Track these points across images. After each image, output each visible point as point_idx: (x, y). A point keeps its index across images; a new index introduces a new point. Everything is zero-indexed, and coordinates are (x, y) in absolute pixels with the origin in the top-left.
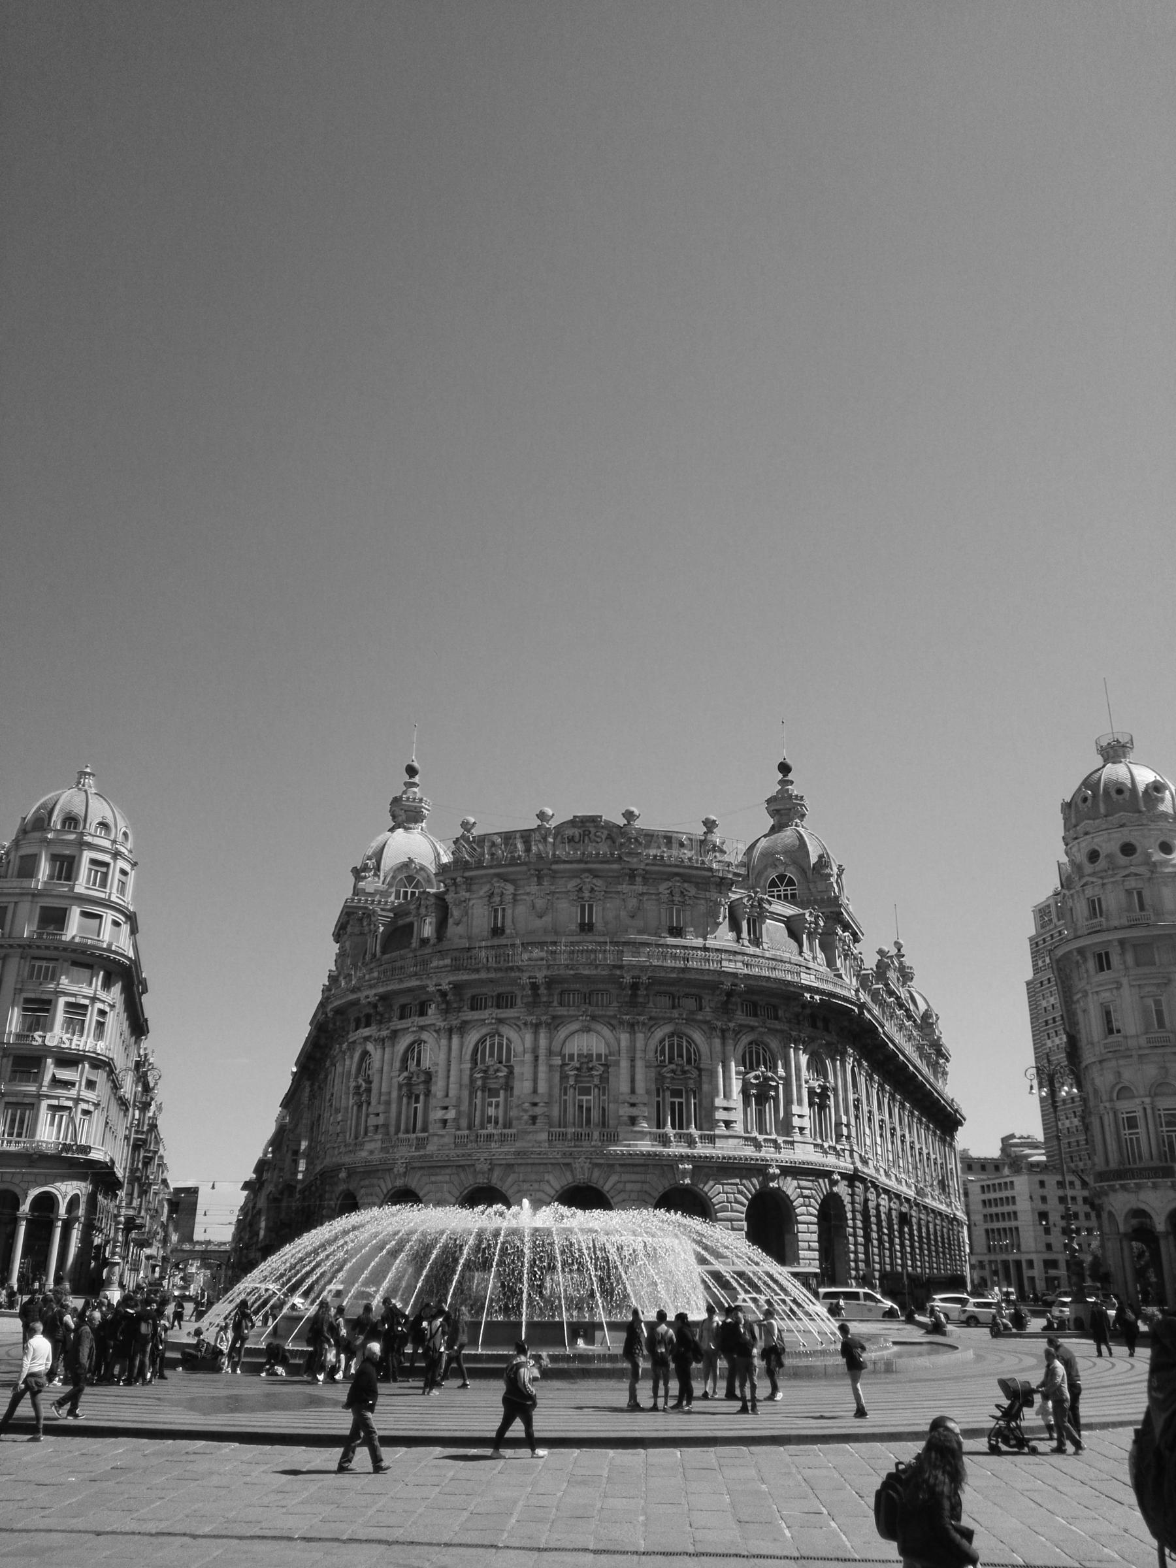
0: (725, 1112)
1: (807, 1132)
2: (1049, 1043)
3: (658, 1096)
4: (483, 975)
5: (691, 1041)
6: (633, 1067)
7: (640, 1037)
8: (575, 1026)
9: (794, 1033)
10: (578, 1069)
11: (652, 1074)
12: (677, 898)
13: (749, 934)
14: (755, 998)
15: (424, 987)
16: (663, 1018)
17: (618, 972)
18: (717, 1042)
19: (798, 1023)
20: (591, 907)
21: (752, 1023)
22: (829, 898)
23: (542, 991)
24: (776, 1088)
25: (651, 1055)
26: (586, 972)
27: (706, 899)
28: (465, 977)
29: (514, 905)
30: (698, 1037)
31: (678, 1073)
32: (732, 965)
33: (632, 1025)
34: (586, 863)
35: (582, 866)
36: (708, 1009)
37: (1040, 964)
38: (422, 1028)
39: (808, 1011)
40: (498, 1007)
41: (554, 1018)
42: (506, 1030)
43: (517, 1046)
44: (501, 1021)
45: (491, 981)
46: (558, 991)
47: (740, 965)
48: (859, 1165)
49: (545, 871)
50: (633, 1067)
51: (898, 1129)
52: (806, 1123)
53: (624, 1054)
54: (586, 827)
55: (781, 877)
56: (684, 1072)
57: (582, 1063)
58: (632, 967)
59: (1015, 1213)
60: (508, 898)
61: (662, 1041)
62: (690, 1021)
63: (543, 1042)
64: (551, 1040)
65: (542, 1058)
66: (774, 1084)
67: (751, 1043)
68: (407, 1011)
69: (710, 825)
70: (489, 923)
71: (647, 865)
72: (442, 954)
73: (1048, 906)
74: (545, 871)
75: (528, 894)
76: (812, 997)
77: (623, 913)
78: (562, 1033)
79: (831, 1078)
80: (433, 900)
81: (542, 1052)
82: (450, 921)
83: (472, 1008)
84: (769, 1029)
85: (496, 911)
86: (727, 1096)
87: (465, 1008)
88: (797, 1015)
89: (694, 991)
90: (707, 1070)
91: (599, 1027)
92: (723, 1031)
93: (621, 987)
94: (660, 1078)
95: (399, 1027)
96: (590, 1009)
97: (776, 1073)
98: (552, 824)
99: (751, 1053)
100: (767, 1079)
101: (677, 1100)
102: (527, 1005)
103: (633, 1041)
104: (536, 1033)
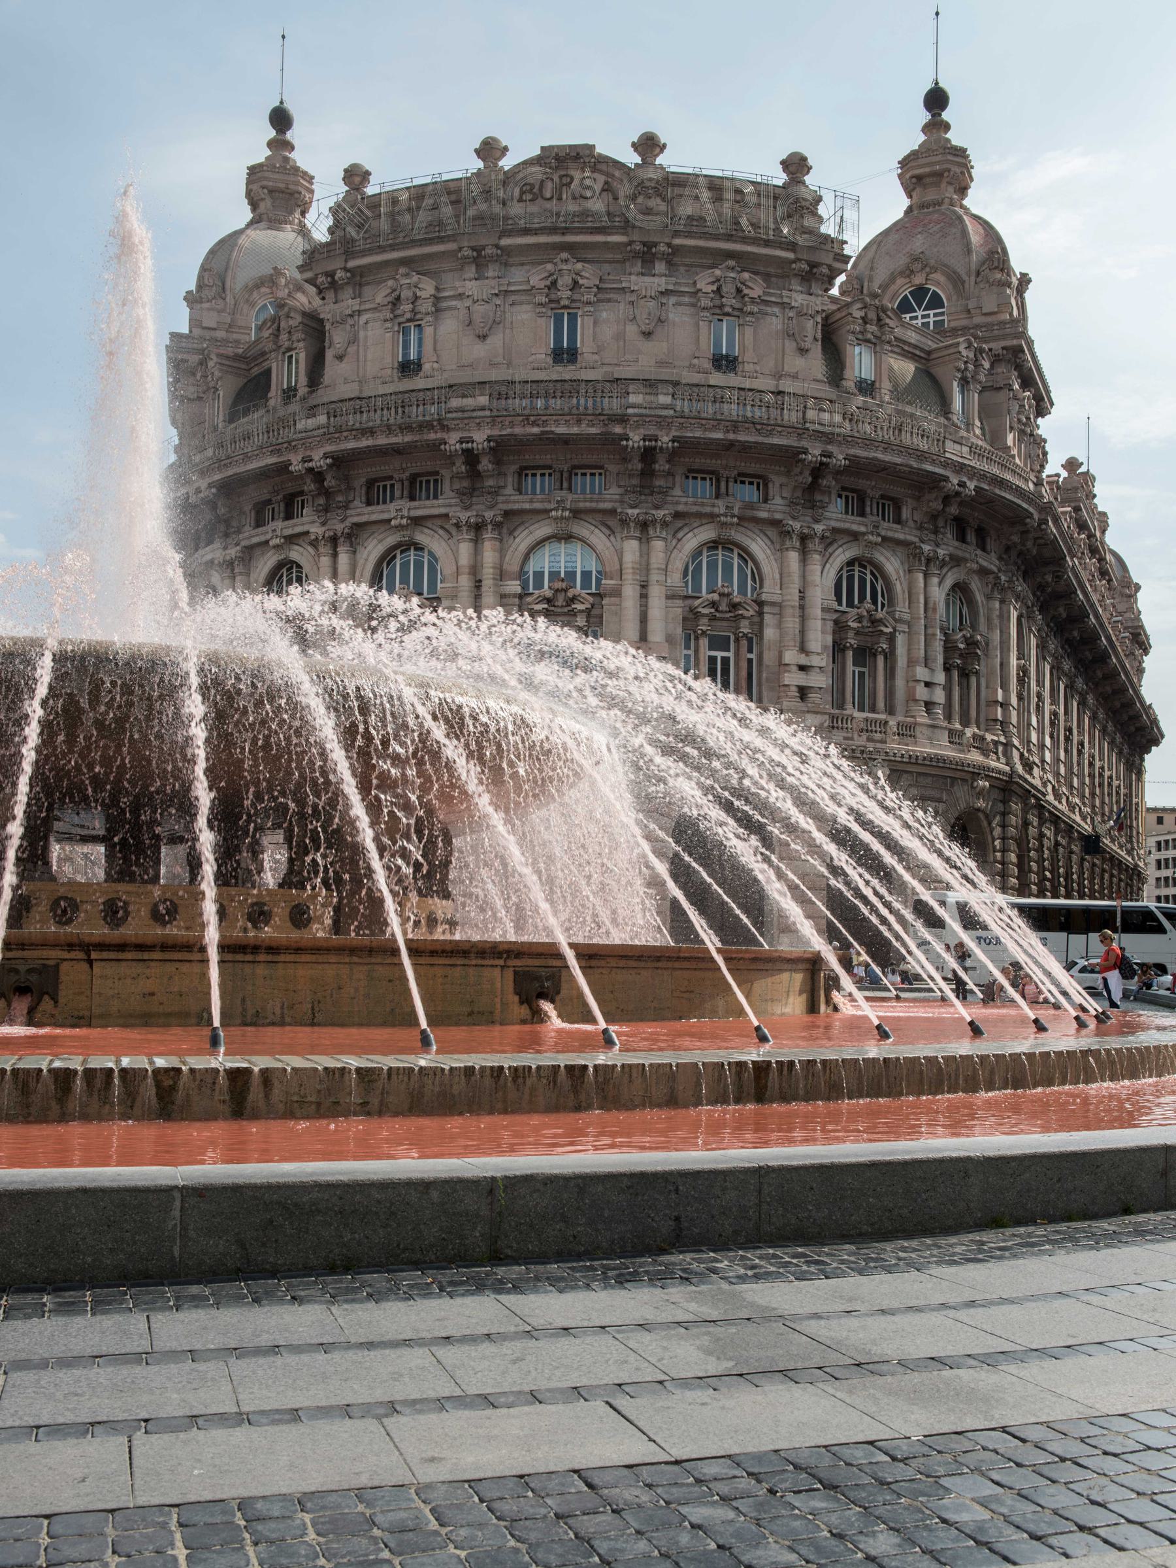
0: (802, 675)
3: (688, 647)
4: (382, 440)
5: (746, 555)
6: (644, 596)
7: (658, 545)
8: (543, 529)
9: (926, 548)
10: (548, 601)
11: (678, 609)
12: (730, 301)
14: (862, 484)
15: (283, 468)
16: (699, 515)
17: (618, 430)
18: (793, 557)
19: (936, 532)
20: (573, 319)
21: (855, 527)
22: (1002, 323)
23: (485, 465)
24: (891, 639)
25: (675, 579)
26: (561, 430)
27: (783, 305)
28: (351, 445)
29: (437, 319)
30: (759, 547)
33: (644, 526)
34: (565, 231)
35: (557, 239)
36: (778, 500)
38: (291, 539)
39: (954, 510)
40: (412, 498)
41: (507, 514)
42: (422, 537)
43: (446, 566)
44: (417, 521)
45: (397, 451)
47: (838, 418)
48: (1019, 768)
49: (489, 251)
50: (644, 596)
51: (1075, 732)
52: (939, 696)
53: (628, 576)
54: (566, 162)
55: (920, 293)
56: (734, 606)
57: (557, 591)
58: (642, 420)
60: (426, 307)
61: (697, 553)
62: (746, 520)
63: (489, 555)
64: (502, 553)
65: (488, 583)
66: (888, 630)
67: (850, 563)
68: (268, 514)
69: (796, 165)
70: (394, 354)
72: (312, 411)
74: (489, 251)
75: (460, 296)
76: (962, 484)
77: (631, 330)
78: (523, 540)
79: (983, 627)
80: (299, 319)
81: (488, 574)
82: (329, 354)
83: (369, 503)
84: (885, 539)
85: (406, 332)
86: (803, 649)
87: (357, 503)
88: (934, 517)
89: (754, 468)
90: (773, 604)
91: (581, 529)
92: (804, 538)
93: (624, 456)
94: (691, 617)
95: (255, 540)
96: (570, 497)
97: (891, 613)
98: (506, 163)
99: (850, 579)
100: (874, 622)
101: (719, 654)
102: (461, 493)
103: (645, 554)
104: (477, 541)
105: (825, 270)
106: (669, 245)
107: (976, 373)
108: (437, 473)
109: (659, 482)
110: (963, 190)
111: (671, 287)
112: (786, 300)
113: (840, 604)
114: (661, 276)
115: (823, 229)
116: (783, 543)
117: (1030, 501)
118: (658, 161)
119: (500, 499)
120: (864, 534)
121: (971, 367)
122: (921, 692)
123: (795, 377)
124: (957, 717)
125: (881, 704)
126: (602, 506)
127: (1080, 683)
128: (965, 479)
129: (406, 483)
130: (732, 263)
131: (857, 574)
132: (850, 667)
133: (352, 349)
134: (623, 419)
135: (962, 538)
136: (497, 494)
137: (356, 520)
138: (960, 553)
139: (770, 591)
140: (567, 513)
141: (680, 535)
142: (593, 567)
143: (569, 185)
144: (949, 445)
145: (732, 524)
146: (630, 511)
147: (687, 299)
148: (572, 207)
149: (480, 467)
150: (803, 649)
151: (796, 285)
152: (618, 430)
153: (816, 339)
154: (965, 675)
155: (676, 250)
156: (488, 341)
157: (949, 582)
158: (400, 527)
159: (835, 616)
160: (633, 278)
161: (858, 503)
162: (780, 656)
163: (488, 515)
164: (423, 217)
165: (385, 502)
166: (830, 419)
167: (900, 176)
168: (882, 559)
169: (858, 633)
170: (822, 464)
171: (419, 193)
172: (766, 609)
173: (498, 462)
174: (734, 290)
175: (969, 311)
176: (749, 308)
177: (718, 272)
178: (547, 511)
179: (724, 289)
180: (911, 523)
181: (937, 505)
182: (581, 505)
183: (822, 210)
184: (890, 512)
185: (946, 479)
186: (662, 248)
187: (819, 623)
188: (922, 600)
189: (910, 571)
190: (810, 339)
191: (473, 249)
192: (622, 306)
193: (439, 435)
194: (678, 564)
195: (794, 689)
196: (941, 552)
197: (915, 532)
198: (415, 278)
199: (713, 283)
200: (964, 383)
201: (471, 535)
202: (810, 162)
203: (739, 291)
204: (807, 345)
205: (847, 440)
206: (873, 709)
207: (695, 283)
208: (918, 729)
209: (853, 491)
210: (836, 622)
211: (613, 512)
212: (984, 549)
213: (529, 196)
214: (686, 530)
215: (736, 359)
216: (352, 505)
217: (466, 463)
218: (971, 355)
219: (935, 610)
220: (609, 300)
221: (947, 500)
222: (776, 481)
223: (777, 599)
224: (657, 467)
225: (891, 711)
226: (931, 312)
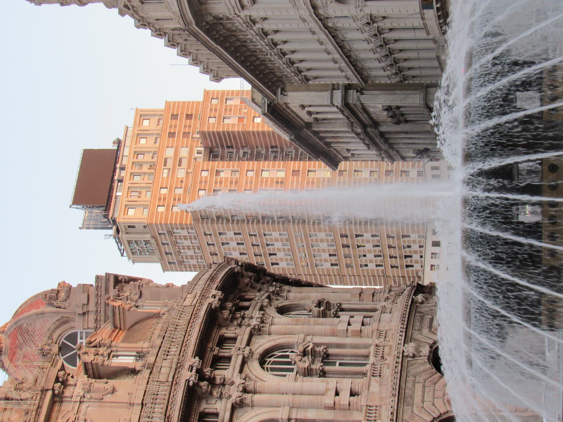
9: (254, 322)
18: (257, 397)
19: (243, 318)
21: (239, 361)
24: (317, 345)
37: (194, 262)
39: (229, 305)
47: (166, 364)
66: (311, 346)
67: (263, 368)
90: (290, 412)
92: (245, 391)
99: (273, 370)
100: (304, 353)
105: (62, 373)
107: (132, 300)
112: (78, 399)
122: (356, 326)
125: (363, 351)
128: (211, 295)
131: (269, 366)
132: (337, 367)
135: (247, 308)
144: (187, 302)
151: (67, 393)
157: (278, 315)
161: (219, 361)
162: (327, 408)
166: (165, 370)
168: (261, 350)
169: (313, 362)
175: (84, 314)
180: (237, 331)
181: (226, 313)
184: (227, 346)
185: (210, 304)
187: (304, 383)
188: (289, 326)
190: (107, 386)
195: (352, 398)
197: (243, 327)
206: (367, 357)
208: (380, 329)
221: (222, 307)
223: (287, 409)
225: (367, 346)
226: (79, 341)
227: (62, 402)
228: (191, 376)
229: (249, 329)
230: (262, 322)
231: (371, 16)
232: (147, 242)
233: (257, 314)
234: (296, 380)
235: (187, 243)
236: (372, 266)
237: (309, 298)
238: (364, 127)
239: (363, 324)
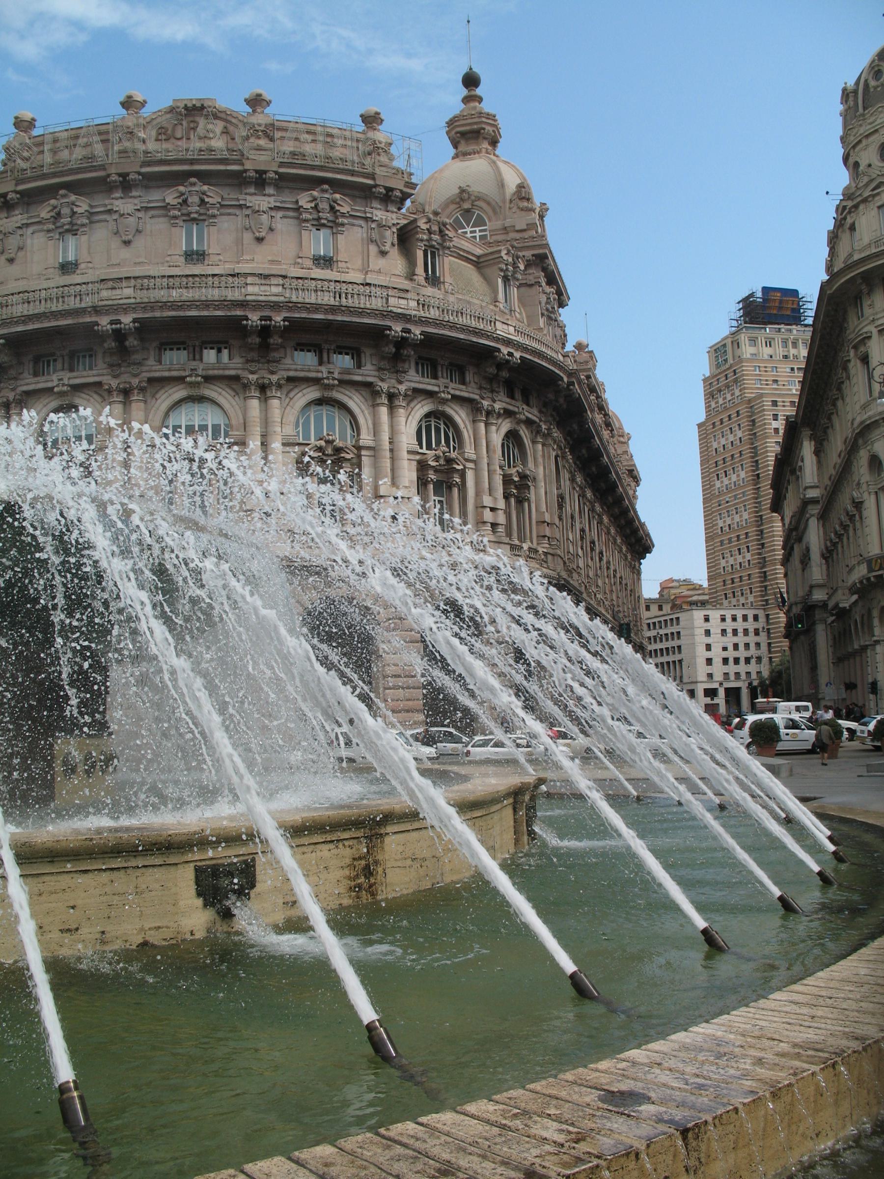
1: (501, 529)
2: (718, 484)
7: (275, 403)
8: (179, 393)
9: (485, 403)
12: (326, 215)
13: (426, 270)
18: (384, 411)
19: (492, 391)
21: (430, 388)
23: (132, 342)
25: (289, 430)
26: (193, 313)
28: (20, 328)
31: (329, 451)
32: (402, 302)
35: (186, 167)
36: (369, 367)
37: (713, 405)
39: (505, 374)
40: (71, 370)
41: (151, 380)
46: (155, 344)
47: (413, 304)
49: (131, 177)
52: (501, 518)
54: (193, 111)
56: (338, 450)
58: (258, 305)
59: (679, 647)
66: (460, 467)
67: (428, 415)
69: (371, 120)
71: (282, 164)
73: (724, 346)
74: (131, 177)
75: (110, 212)
77: (248, 237)
79: (531, 465)
83: (36, 374)
87: (26, 375)
90: (368, 448)
92: (391, 397)
97: (462, 454)
98: (146, 112)
100: (449, 461)
102: (111, 366)
104: (124, 403)
105: (398, 194)
106: (276, 173)
107: (514, 272)
108: (91, 349)
109: (276, 355)
110: (494, 143)
111: (278, 204)
112: (369, 215)
113: (421, 448)
114: (269, 196)
115: (395, 164)
116: (374, 399)
117: (561, 368)
118: (268, 110)
119: (145, 368)
120: (437, 393)
121: (511, 268)
122: (488, 516)
123: (379, 272)
124: (515, 535)
126: (227, 373)
127: (598, 508)
128: (512, 351)
129: (66, 358)
130: (326, 187)
133: (20, 254)
134: (242, 304)
135: (512, 397)
136: (140, 364)
137: (25, 388)
138: (511, 408)
139: (366, 439)
140: (199, 379)
141: (291, 395)
142: (221, 420)
143: (194, 129)
145: (333, 386)
146: (251, 377)
147: (291, 214)
148: (199, 145)
149: (127, 343)
150: (394, 483)
151: (376, 204)
152: (239, 313)
153: (393, 245)
154: (520, 501)
155: (282, 177)
156: (133, 245)
158: (62, 394)
159: (418, 457)
160: (248, 198)
163: (135, 382)
164: (79, 153)
165: (49, 374)
167: (447, 133)
168: (449, 411)
170: (403, 338)
171: (75, 135)
172: (363, 452)
173: (142, 340)
174: (327, 207)
176: (340, 220)
177: (315, 193)
178: (181, 380)
179: (321, 206)
180: (473, 384)
181: (492, 370)
182: (211, 372)
183: (393, 150)
185: (499, 350)
186: (272, 175)
188: (484, 444)
189: (474, 421)
190: (388, 245)
191: (120, 175)
192: (240, 218)
193: (94, 319)
194: (291, 417)
196: (497, 406)
197: (478, 392)
198: (73, 198)
199: (311, 201)
200: (506, 279)
201: (121, 398)
202: (382, 116)
203: (332, 208)
204: (387, 248)
205: (421, 321)
207: (297, 202)
209: (428, 359)
210: (419, 462)
211: (236, 378)
212: (528, 405)
213: (164, 137)
214: (296, 391)
215: (331, 259)
216: (21, 376)
217: (115, 340)
218: (510, 260)
219: (494, 451)
220: (229, 214)
222: (367, 353)
223: (371, 443)
224: (272, 341)
226: (477, 229)
227: (366, 198)
228: (396, 332)
229: (477, 397)
230: (489, 413)
231: (862, 503)
232: (726, 361)
233: (497, 406)
234: (409, 452)
235: (729, 397)
236: (723, 563)
237: (536, 465)
238: (796, 529)
239: (494, 525)
